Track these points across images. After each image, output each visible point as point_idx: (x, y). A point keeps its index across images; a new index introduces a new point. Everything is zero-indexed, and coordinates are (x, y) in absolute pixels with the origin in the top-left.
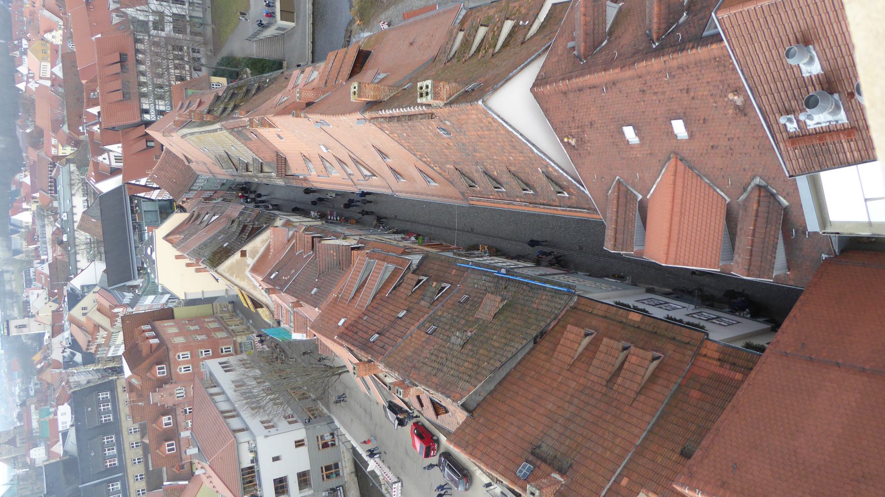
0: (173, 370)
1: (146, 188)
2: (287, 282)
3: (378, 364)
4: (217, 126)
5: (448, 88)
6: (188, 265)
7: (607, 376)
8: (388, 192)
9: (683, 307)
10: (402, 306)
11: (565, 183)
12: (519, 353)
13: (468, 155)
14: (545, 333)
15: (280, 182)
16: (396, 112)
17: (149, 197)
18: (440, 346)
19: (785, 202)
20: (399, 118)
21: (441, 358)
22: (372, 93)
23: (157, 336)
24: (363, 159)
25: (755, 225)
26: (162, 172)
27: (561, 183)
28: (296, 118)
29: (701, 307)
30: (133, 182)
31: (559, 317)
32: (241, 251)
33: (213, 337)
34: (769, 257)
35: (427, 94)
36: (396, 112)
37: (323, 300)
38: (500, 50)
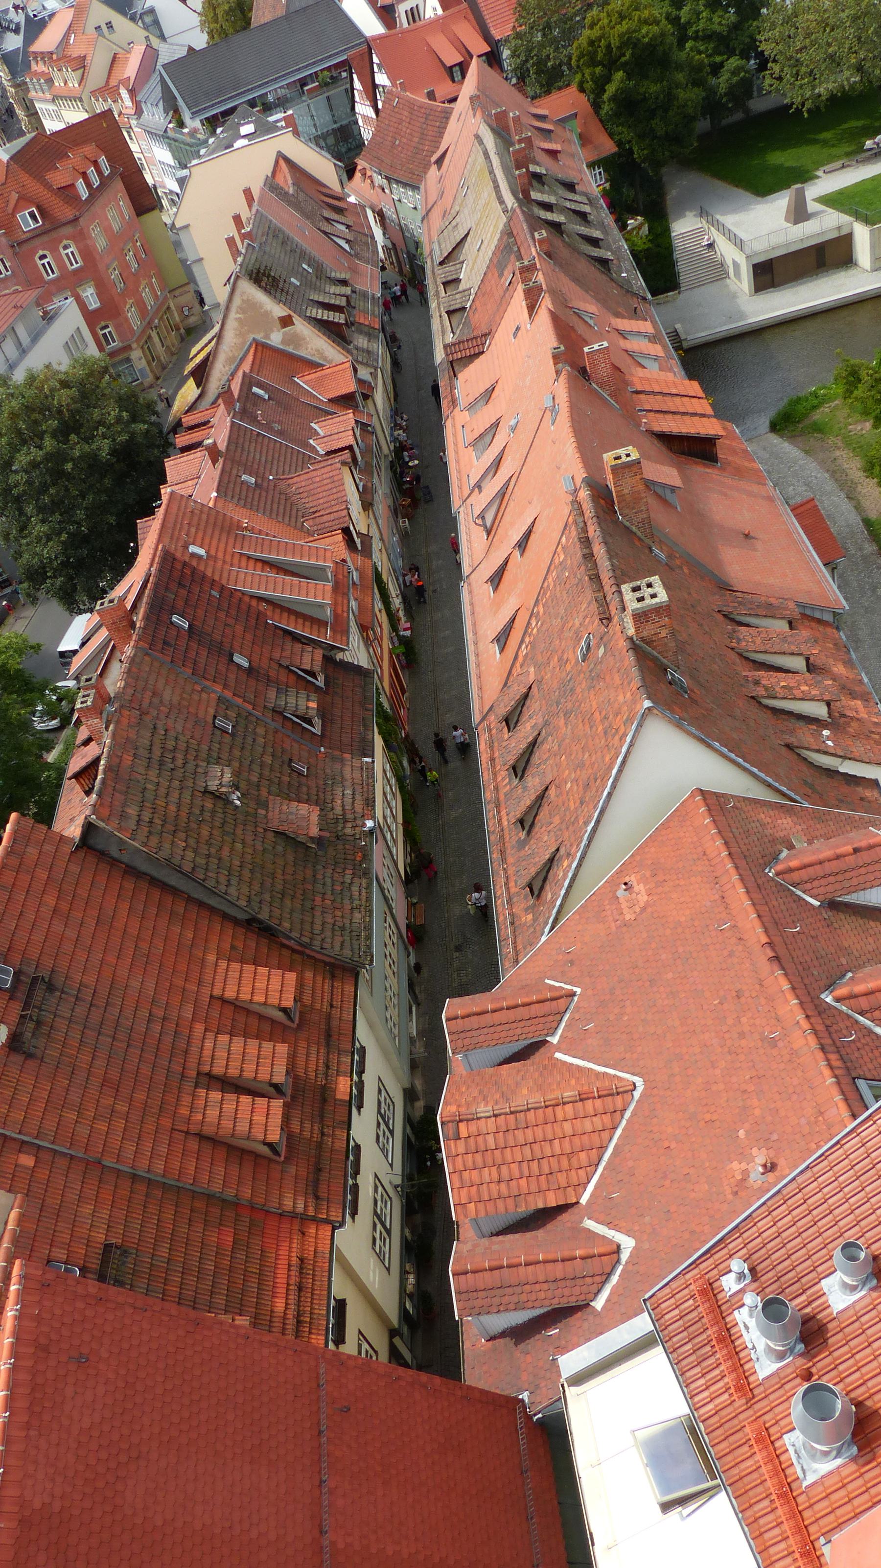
0: (36, 242)
1: (372, 89)
2: (254, 420)
3: (132, 643)
4: (510, 201)
5: (663, 635)
6: (237, 219)
7: (218, 1070)
8: (466, 569)
9: (391, 1165)
10: (256, 658)
11: (549, 896)
12: (218, 899)
13: (558, 703)
14: (273, 935)
15: (439, 355)
16: (599, 551)
17: (357, 98)
18: (197, 751)
19: (599, 1304)
20: (589, 557)
21: (174, 759)
22: (626, 491)
23: (94, 193)
24: (511, 503)
25: (545, 1262)
26: (406, 113)
27: (547, 887)
28: (550, 356)
29: (401, 1196)
30: (375, 59)
31: (307, 951)
32: (290, 316)
33: (126, 303)
34: (496, 1301)
35: (641, 599)
36: (599, 551)
37: (235, 500)
38: (767, 707)
